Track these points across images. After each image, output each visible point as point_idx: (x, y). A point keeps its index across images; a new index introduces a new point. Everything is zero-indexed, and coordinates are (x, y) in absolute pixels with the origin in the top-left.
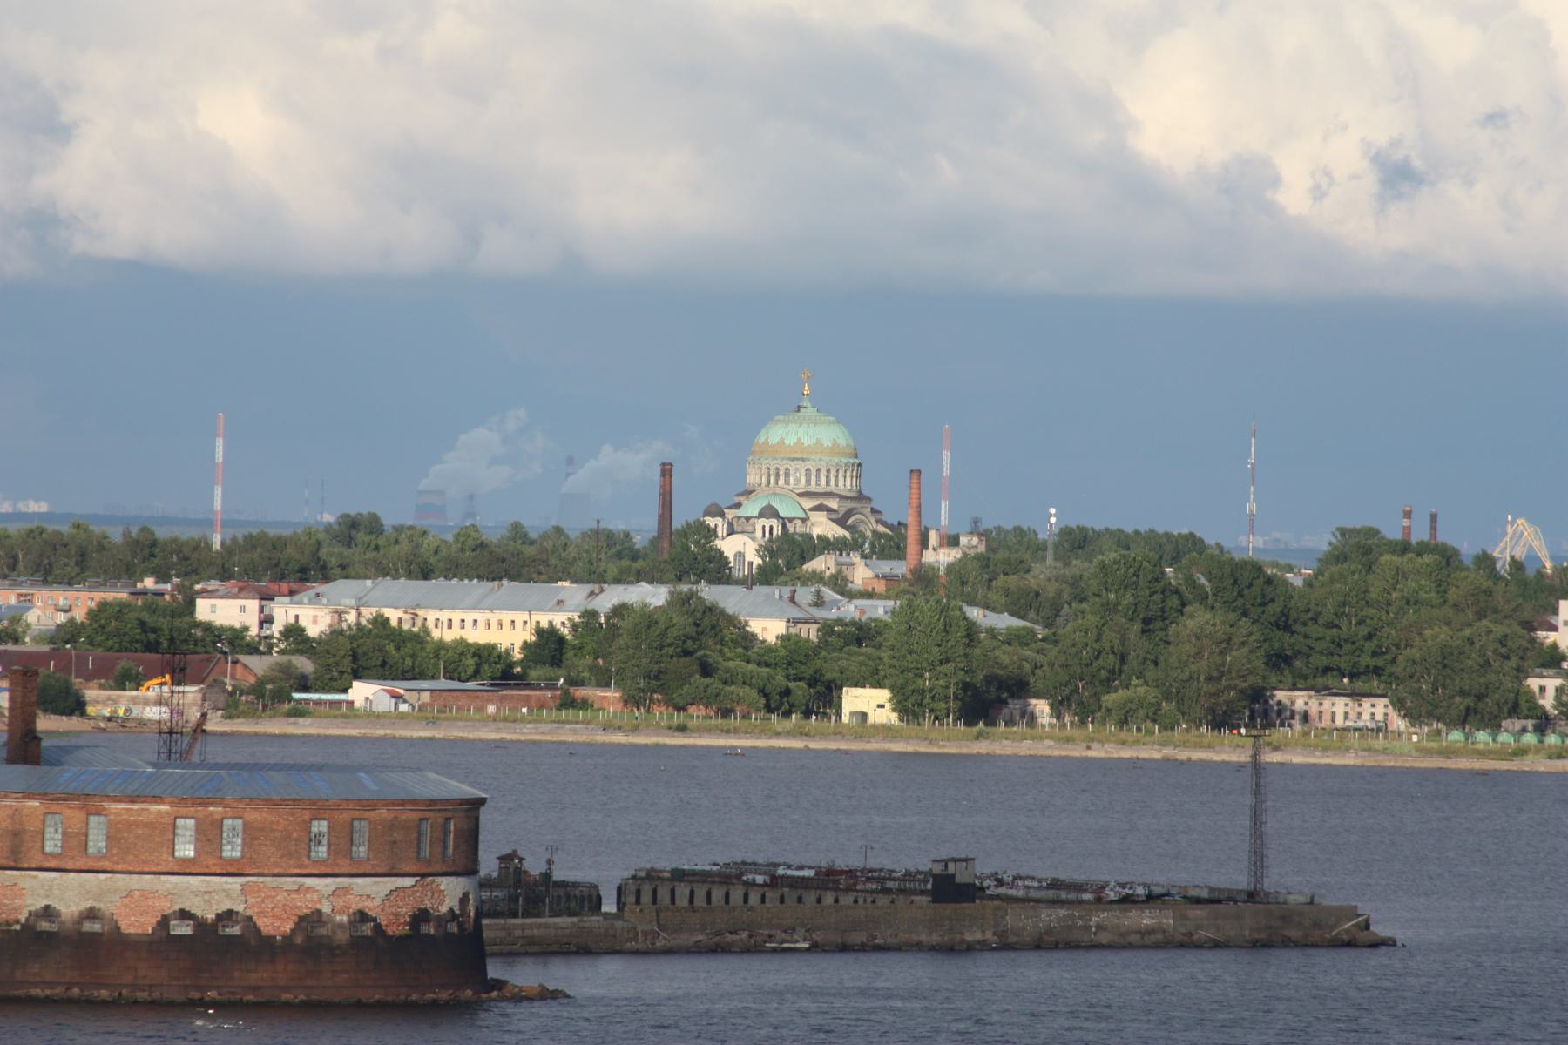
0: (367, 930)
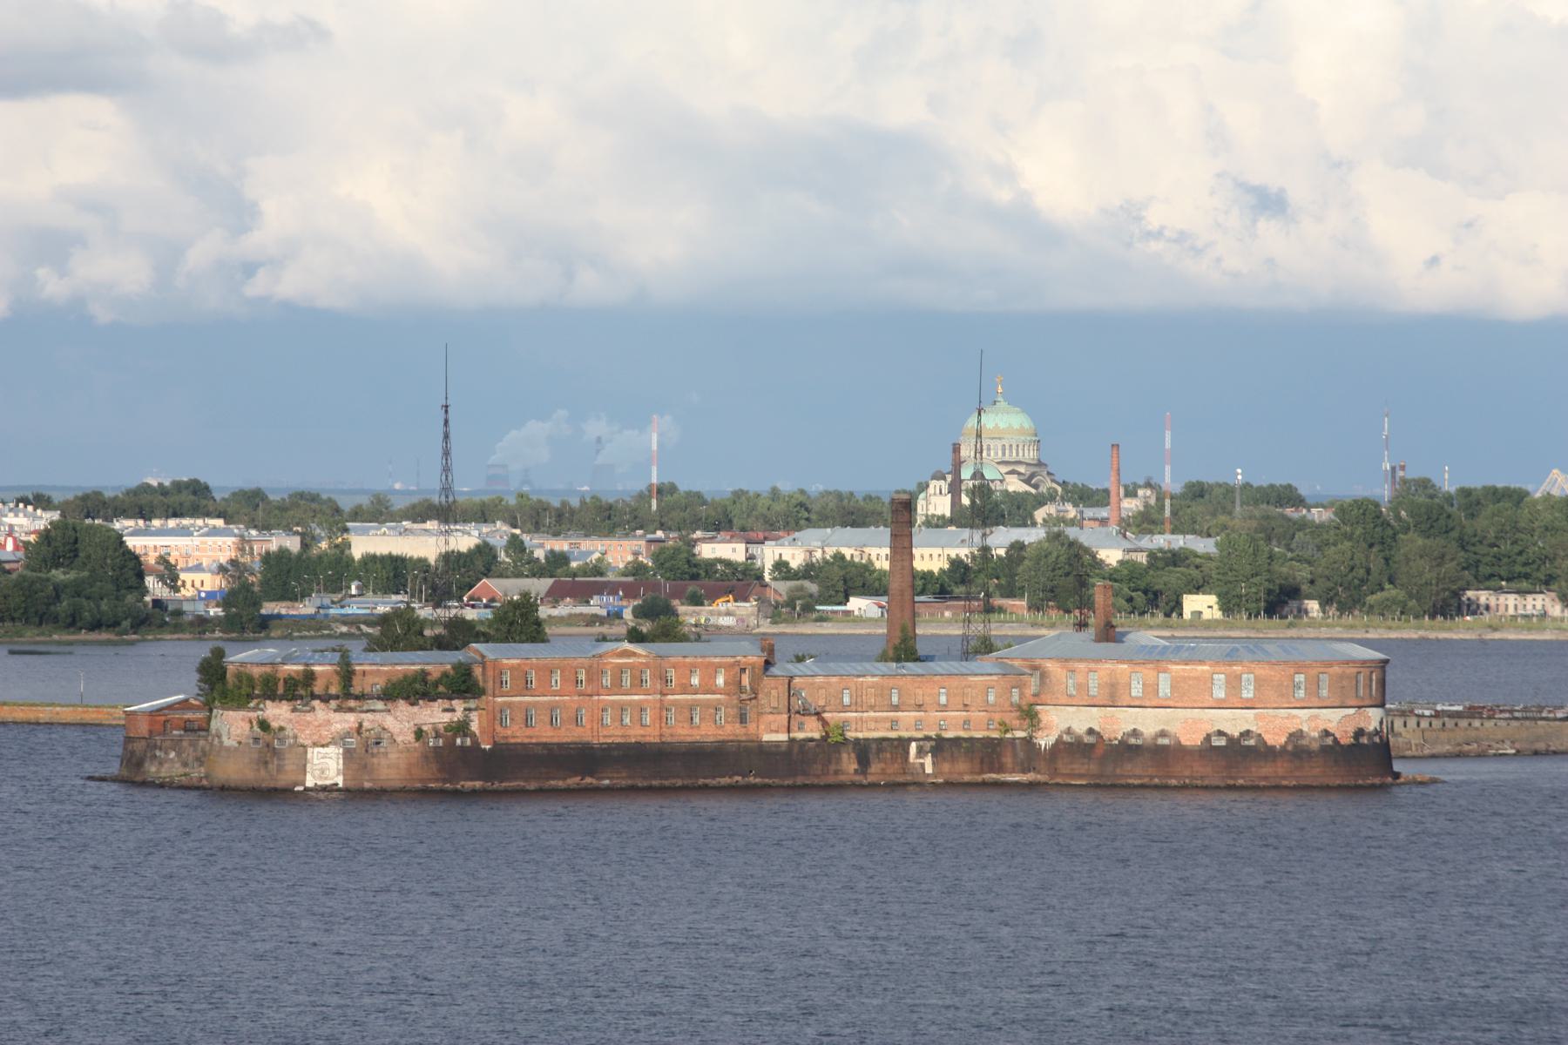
0: (1329, 741)
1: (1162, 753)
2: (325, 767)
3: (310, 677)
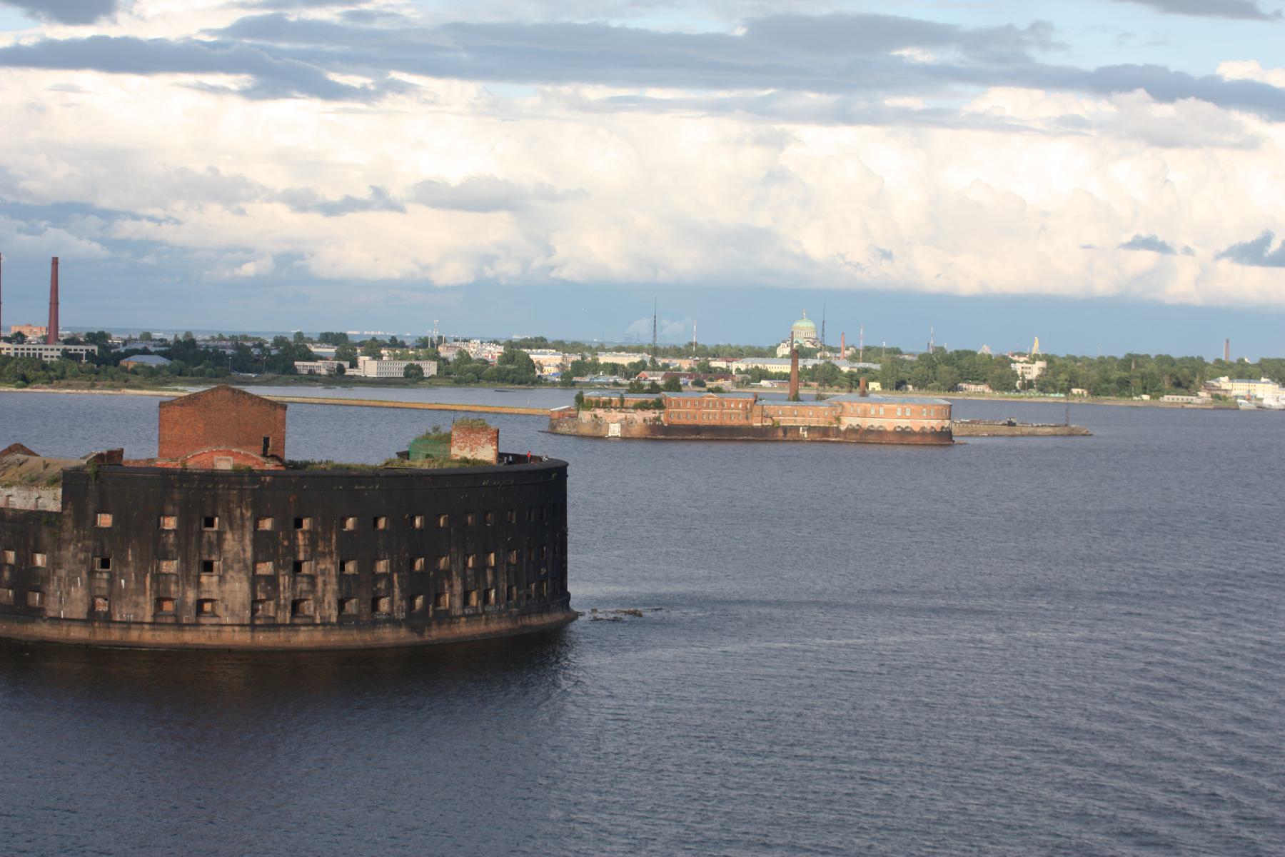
1: (881, 433)
2: (615, 430)
3: (611, 401)
